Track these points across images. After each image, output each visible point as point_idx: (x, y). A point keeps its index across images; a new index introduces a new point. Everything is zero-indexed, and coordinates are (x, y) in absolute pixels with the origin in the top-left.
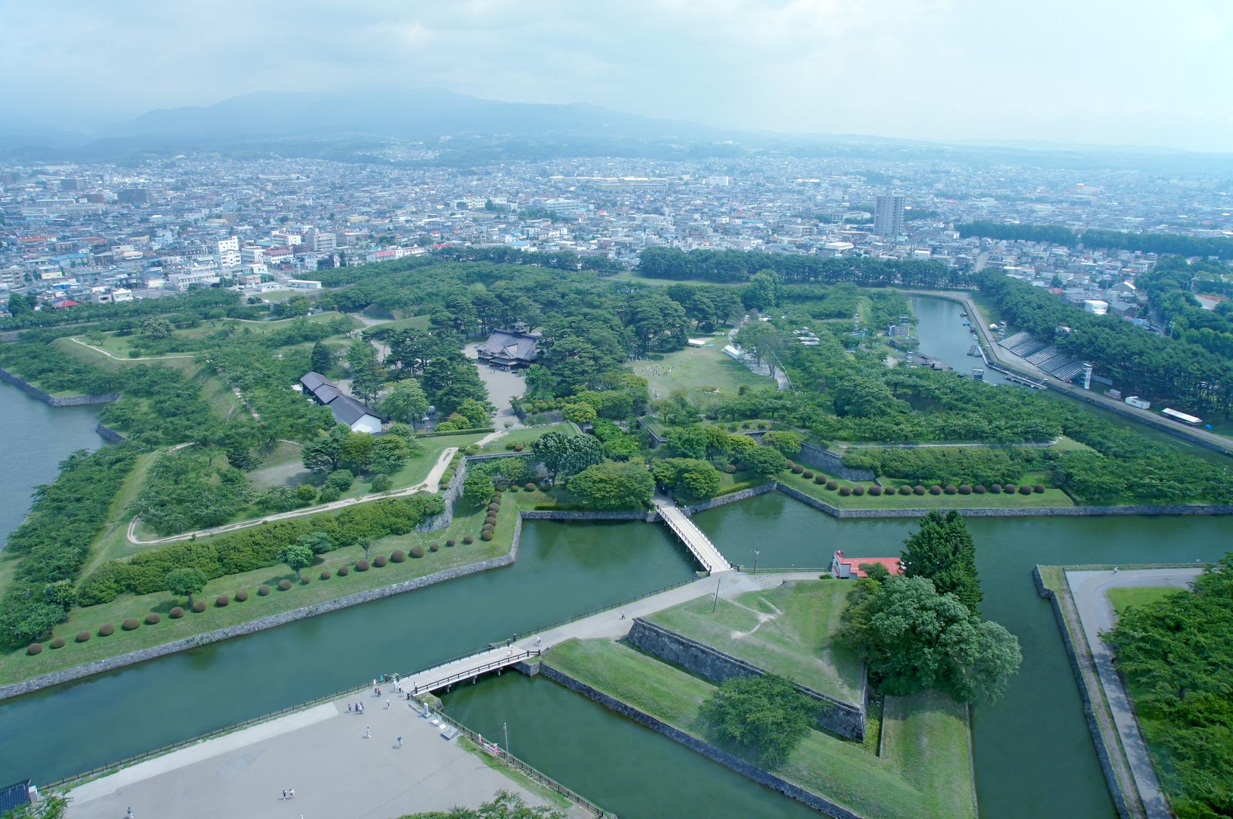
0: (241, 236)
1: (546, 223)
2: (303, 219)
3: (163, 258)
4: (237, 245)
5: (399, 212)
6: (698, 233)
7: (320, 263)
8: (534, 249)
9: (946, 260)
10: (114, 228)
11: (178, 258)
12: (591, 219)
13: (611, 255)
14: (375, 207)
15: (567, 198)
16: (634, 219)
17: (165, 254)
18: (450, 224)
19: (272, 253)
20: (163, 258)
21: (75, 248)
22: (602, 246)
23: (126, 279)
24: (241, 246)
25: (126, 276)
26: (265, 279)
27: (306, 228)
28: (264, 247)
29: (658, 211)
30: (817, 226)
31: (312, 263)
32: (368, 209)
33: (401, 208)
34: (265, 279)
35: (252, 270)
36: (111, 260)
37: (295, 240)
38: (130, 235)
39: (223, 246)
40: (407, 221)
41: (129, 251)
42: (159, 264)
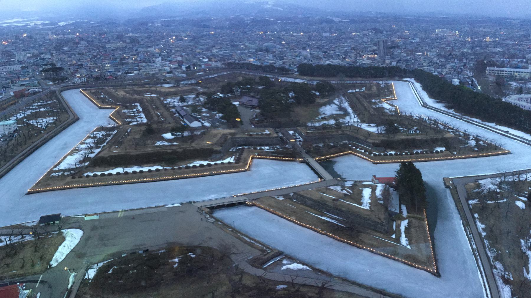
0: (163, 57)
1: (264, 54)
2: (183, 51)
3: (139, 64)
4: (161, 60)
5: (214, 48)
6: (318, 58)
7: (186, 68)
8: (260, 64)
9: (401, 65)
10: (127, 53)
11: (144, 64)
12: (280, 52)
13: (287, 67)
14: (206, 46)
15: (272, 43)
16: (296, 52)
17: (140, 63)
18: (232, 53)
19: (172, 63)
20: (139, 64)
21: (117, 59)
22: (284, 63)
23: (127, 70)
24: (162, 60)
25: (127, 69)
26: (168, 73)
27: (183, 54)
28: (170, 61)
29: (304, 48)
30: (359, 53)
31: (184, 68)
32: (203, 47)
33: (214, 46)
34: (168, 73)
35: (165, 69)
36: (125, 64)
37: (179, 59)
38: (131, 55)
39: (157, 60)
40: (216, 52)
41: (130, 61)
42: (138, 66)
